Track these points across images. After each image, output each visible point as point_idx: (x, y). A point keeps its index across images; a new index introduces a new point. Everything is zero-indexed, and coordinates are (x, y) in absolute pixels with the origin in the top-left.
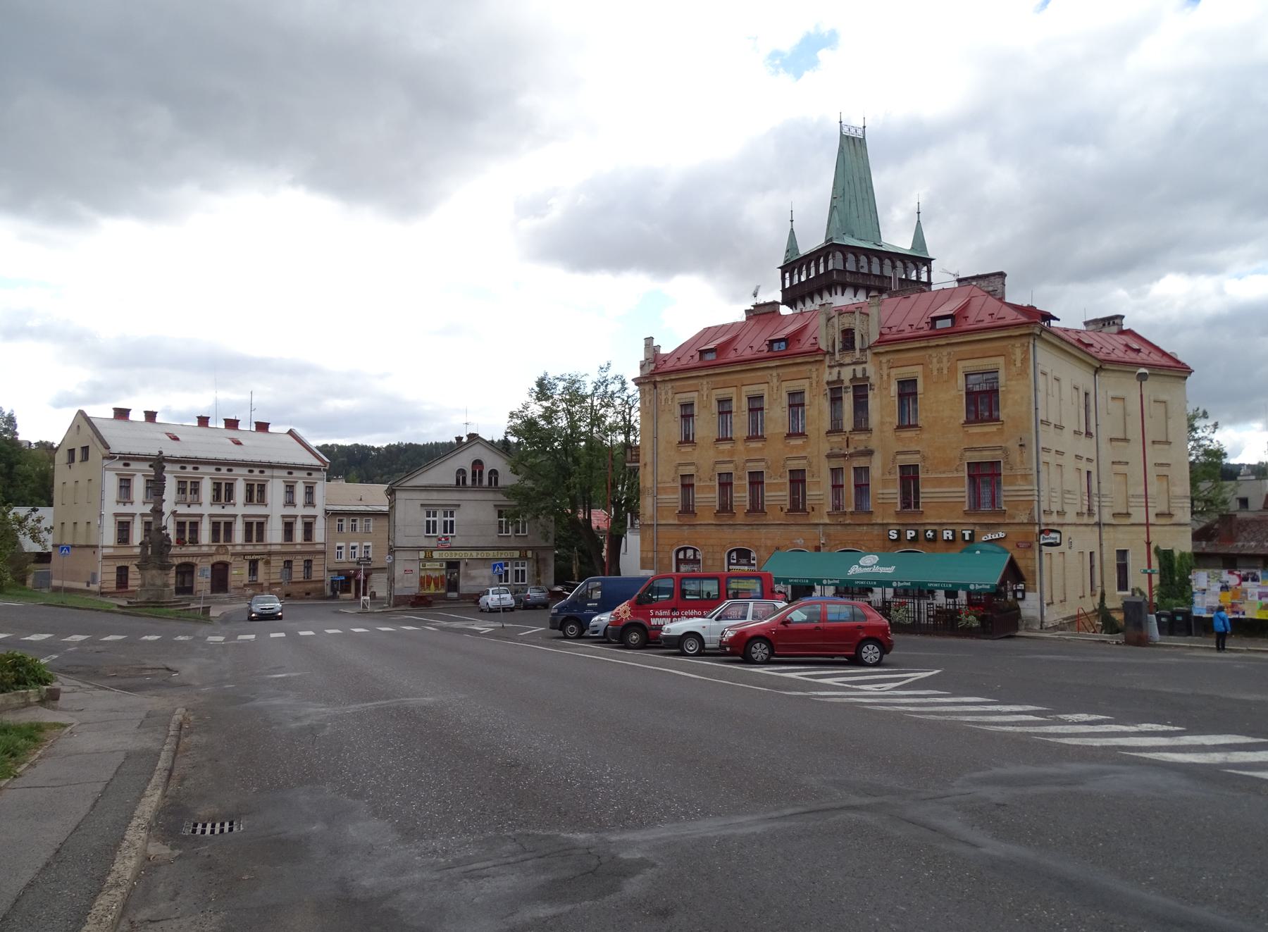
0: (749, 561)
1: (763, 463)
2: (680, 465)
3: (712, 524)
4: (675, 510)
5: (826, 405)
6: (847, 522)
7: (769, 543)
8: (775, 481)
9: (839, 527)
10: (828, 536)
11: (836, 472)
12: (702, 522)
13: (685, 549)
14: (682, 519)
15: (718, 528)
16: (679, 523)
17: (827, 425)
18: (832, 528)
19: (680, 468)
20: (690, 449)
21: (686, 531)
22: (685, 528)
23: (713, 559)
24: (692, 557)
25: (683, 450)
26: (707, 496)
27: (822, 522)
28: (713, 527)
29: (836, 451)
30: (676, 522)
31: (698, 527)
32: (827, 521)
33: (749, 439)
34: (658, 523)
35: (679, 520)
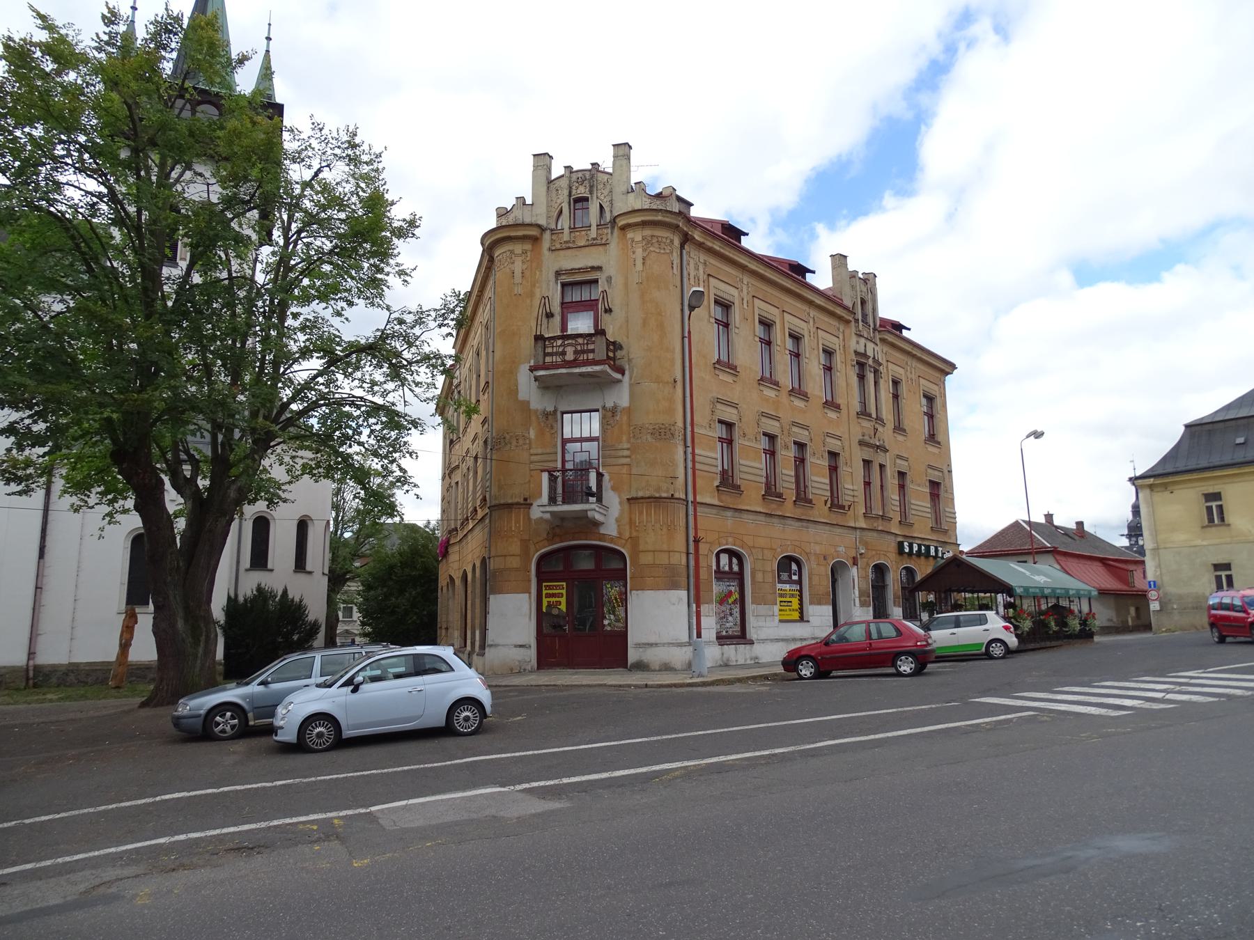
0: (790, 577)
1: (806, 433)
2: (719, 401)
3: (760, 512)
4: (714, 479)
5: (854, 380)
6: (880, 528)
7: (818, 549)
8: (818, 462)
9: (875, 534)
10: (866, 544)
11: (867, 463)
12: (748, 508)
13: (732, 553)
14: (723, 497)
15: (768, 519)
16: (721, 504)
17: (857, 407)
18: (870, 534)
19: (719, 406)
20: (729, 379)
21: (729, 521)
22: (729, 513)
23: (764, 572)
24: (727, 568)
25: (723, 377)
26: (752, 466)
27: (857, 526)
28: (762, 518)
29: (867, 438)
30: (716, 502)
31: (745, 516)
32: (864, 526)
33: (792, 392)
34: (699, 499)
35: (720, 500)
